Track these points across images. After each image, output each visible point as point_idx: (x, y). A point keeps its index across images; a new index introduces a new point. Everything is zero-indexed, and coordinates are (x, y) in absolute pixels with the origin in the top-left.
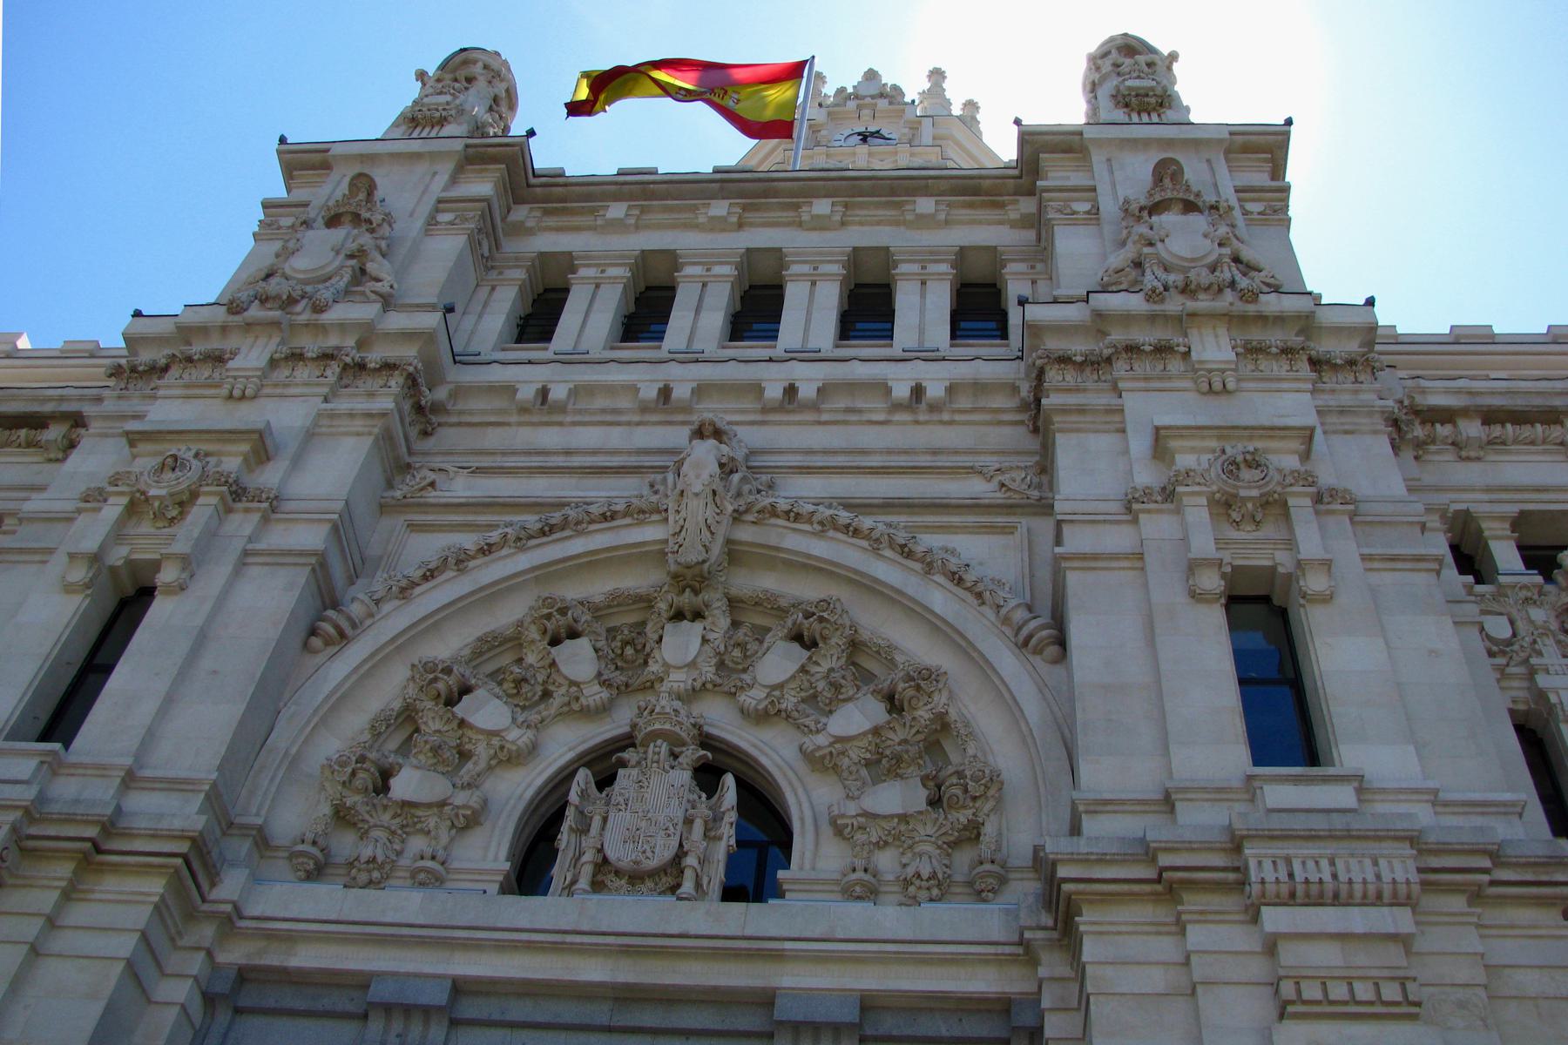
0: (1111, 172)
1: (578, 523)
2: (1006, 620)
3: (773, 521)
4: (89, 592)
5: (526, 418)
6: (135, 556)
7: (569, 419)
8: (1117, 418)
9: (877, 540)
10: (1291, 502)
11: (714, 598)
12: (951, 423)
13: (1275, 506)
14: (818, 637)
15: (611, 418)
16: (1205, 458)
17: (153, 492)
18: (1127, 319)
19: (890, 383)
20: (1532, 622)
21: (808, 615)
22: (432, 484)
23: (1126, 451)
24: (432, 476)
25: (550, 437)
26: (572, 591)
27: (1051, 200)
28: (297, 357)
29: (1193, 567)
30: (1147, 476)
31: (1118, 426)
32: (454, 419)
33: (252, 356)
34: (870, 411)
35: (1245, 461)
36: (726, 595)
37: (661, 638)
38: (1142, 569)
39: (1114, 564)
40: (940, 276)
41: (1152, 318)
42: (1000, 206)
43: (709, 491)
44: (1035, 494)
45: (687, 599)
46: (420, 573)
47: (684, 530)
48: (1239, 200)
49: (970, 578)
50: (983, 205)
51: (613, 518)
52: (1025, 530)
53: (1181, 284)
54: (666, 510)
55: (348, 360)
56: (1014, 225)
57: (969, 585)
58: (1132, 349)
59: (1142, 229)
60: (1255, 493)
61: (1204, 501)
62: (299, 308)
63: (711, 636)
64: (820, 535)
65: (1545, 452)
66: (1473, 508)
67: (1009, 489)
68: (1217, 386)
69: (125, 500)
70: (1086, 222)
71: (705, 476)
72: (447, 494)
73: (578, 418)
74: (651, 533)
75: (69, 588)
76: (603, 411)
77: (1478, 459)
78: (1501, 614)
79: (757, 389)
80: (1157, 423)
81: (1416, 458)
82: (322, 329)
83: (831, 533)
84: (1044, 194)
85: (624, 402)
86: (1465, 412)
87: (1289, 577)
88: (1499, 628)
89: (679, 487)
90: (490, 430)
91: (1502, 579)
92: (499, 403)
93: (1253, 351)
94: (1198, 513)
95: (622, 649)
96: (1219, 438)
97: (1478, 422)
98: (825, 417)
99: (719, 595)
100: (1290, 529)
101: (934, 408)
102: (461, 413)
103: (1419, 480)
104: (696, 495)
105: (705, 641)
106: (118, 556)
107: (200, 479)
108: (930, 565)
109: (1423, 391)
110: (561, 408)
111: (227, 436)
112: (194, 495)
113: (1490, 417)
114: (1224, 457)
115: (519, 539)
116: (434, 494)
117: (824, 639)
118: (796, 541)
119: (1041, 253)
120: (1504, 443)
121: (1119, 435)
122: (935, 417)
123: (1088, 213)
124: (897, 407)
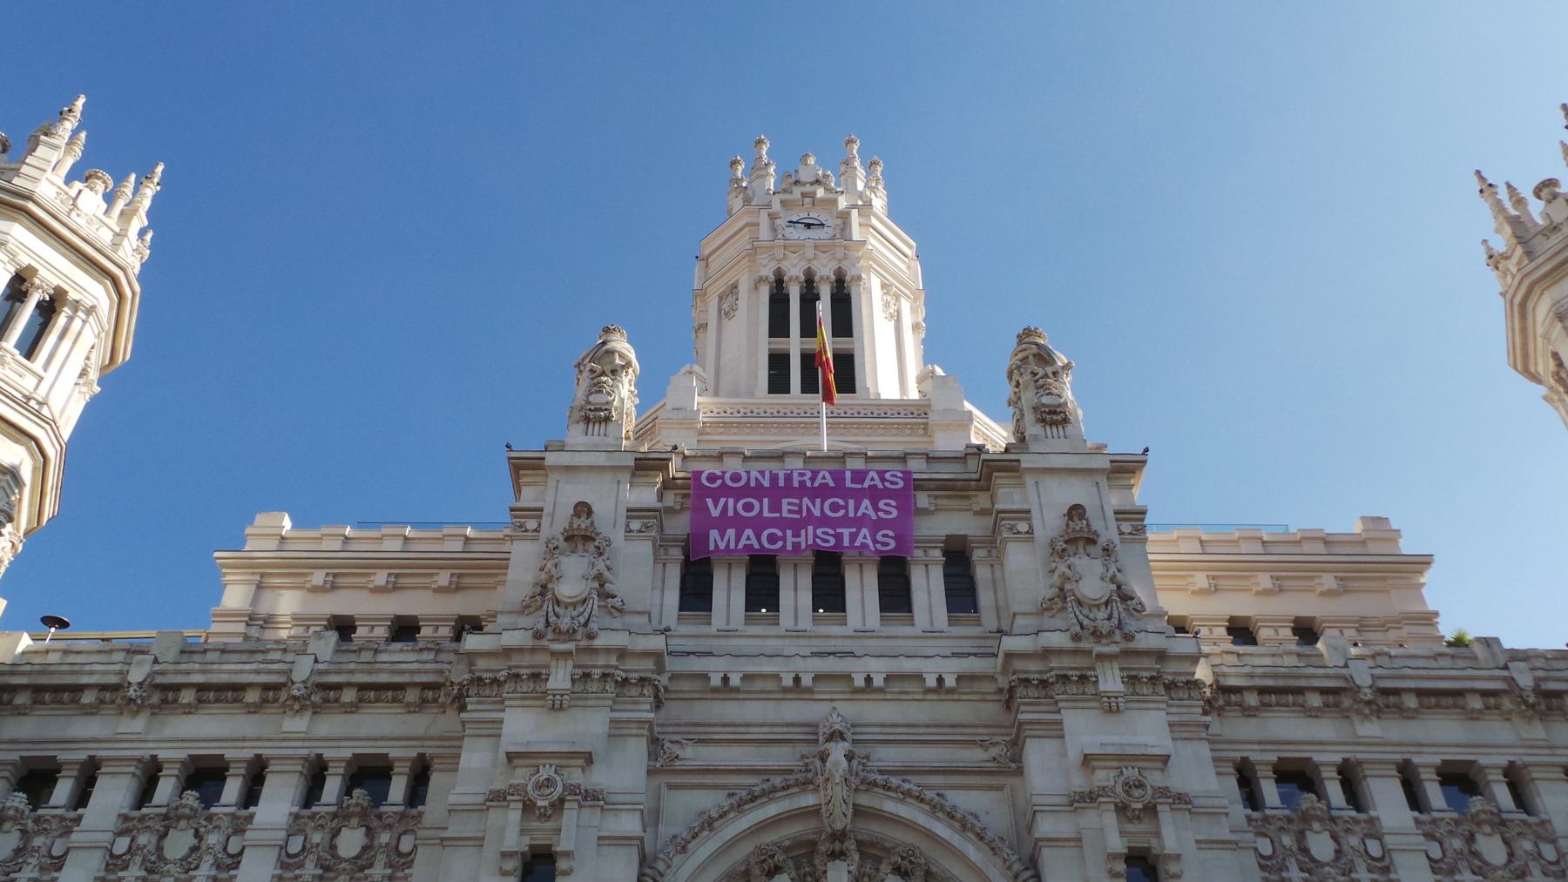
0: (1039, 496)
1: (770, 792)
2: (1009, 868)
3: (875, 789)
4: (515, 874)
5: (716, 695)
6: (533, 842)
7: (741, 696)
8: (1059, 727)
9: (934, 807)
10: (1159, 808)
11: (850, 845)
12: (959, 700)
13: (1151, 810)
14: (909, 871)
15: (764, 696)
16: (1112, 773)
17: (540, 803)
18: (1060, 652)
19: (924, 676)
20: (1284, 846)
21: (903, 858)
22: (677, 757)
23: (1064, 754)
24: (676, 750)
25: (731, 710)
26: (769, 838)
27: (1003, 519)
28: (586, 676)
29: (1113, 857)
30: (1079, 782)
31: (1060, 733)
32: (673, 696)
33: (560, 678)
34: (913, 692)
35: (1134, 784)
36: (855, 839)
37: (825, 872)
38: (1081, 847)
39: (1067, 844)
40: (936, 562)
41: (1076, 652)
42: (968, 497)
43: (843, 779)
44: (1014, 766)
45: (837, 846)
46: (690, 836)
47: (832, 802)
48: (1117, 520)
49: (989, 835)
50: (956, 497)
51: (788, 788)
52: (1009, 790)
53: (1092, 629)
54: (818, 786)
55: (619, 679)
56: (976, 513)
57: (986, 841)
58: (1064, 678)
59: (1062, 568)
60: (1140, 806)
61: (1113, 807)
62: (579, 636)
63: (852, 868)
64: (902, 801)
65: (1293, 711)
66: (1254, 757)
67: (999, 762)
68: (1115, 708)
69: (520, 805)
70: (1026, 540)
71: (841, 770)
72: (686, 763)
73: (746, 696)
74: (809, 800)
75: (504, 873)
76: (762, 692)
77: (1255, 716)
78: (1266, 836)
79: (847, 677)
80: (1086, 752)
81: (1219, 715)
82: (594, 651)
83: (908, 799)
84: (999, 515)
85: (770, 685)
86: (1249, 689)
87: (1157, 857)
88: (1265, 847)
89: (826, 775)
90: (696, 702)
91: (1266, 811)
92: (696, 685)
93: (1132, 680)
94: (1110, 819)
95: (805, 875)
96: (1119, 760)
97: (1256, 693)
98: (888, 697)
99: (853, 841)
100: (1158, 826)
101: (950, 691)
102: (676, 692)
103: (1220, 735)
104: (838, 784)
105: (849, 872)
106: (523, 844)
107: (564, 790)
108: (964, 827)
109: (1224, 675)
110: (736, 690)
111: (570, 755)
112: (562, 800)
113: (1263, 691)
114: (1122, 779)
115: (739, 806)
116: (681, 763)
117: (913, 874)
118: (890, 806)
119: (993, 543)
120: (1270, 706)
121: (1060, 740)
122: (950, 697)
123: (1027, 533)
124: (929, 691)
